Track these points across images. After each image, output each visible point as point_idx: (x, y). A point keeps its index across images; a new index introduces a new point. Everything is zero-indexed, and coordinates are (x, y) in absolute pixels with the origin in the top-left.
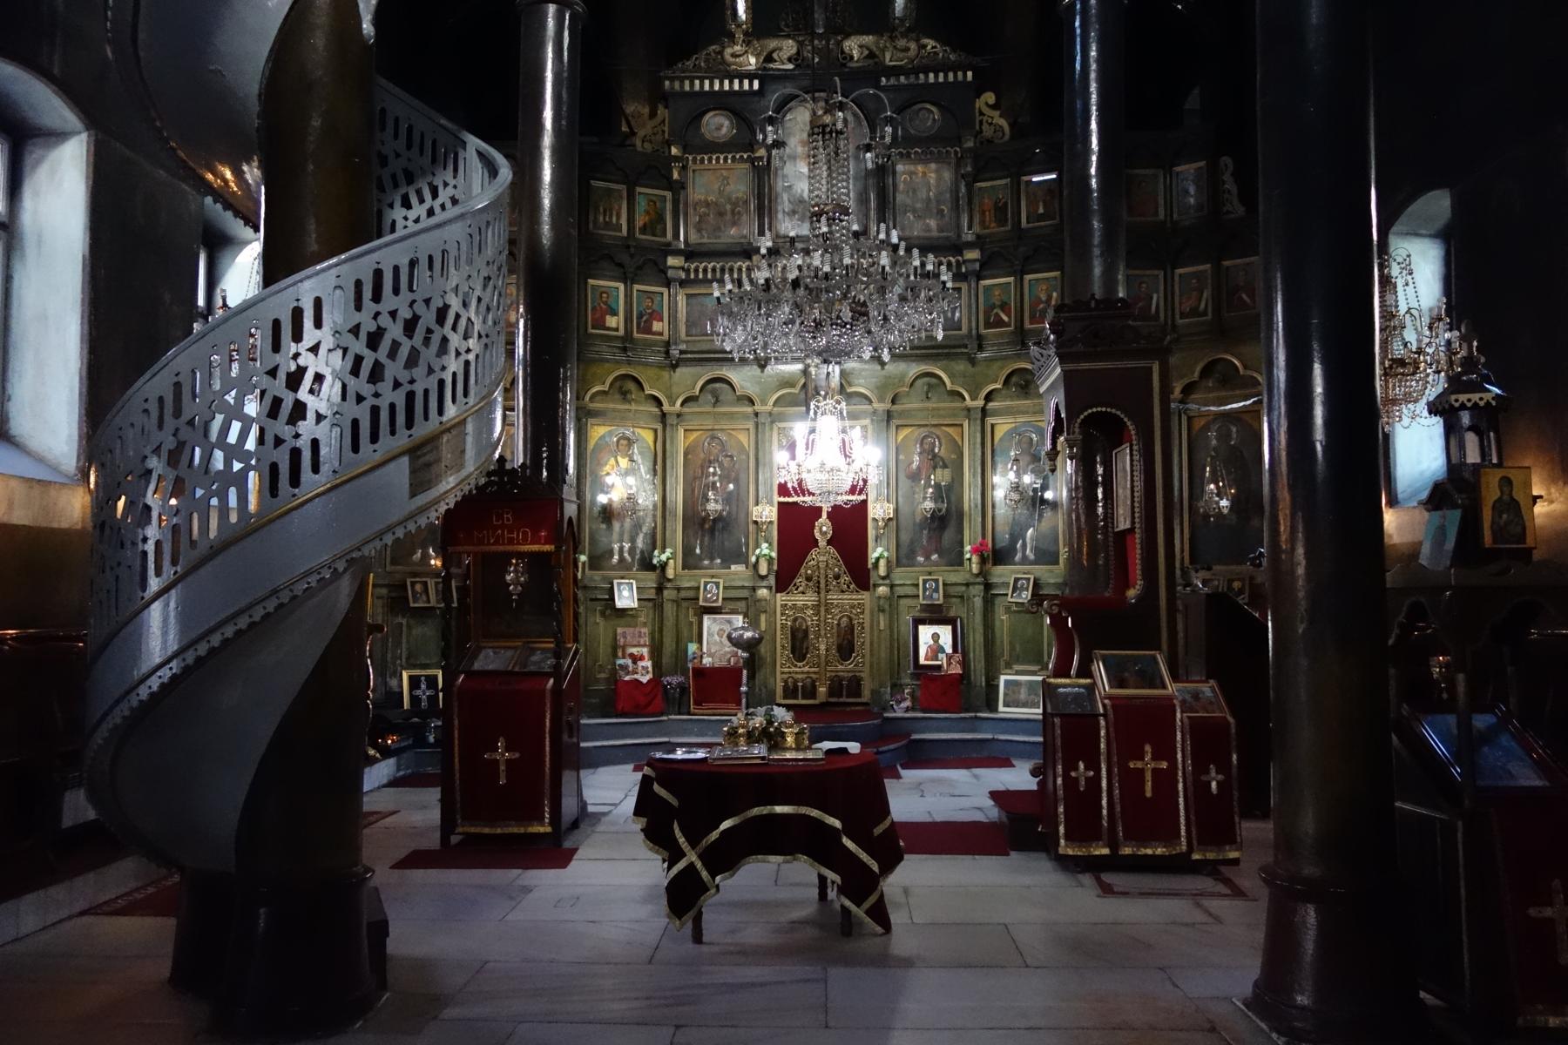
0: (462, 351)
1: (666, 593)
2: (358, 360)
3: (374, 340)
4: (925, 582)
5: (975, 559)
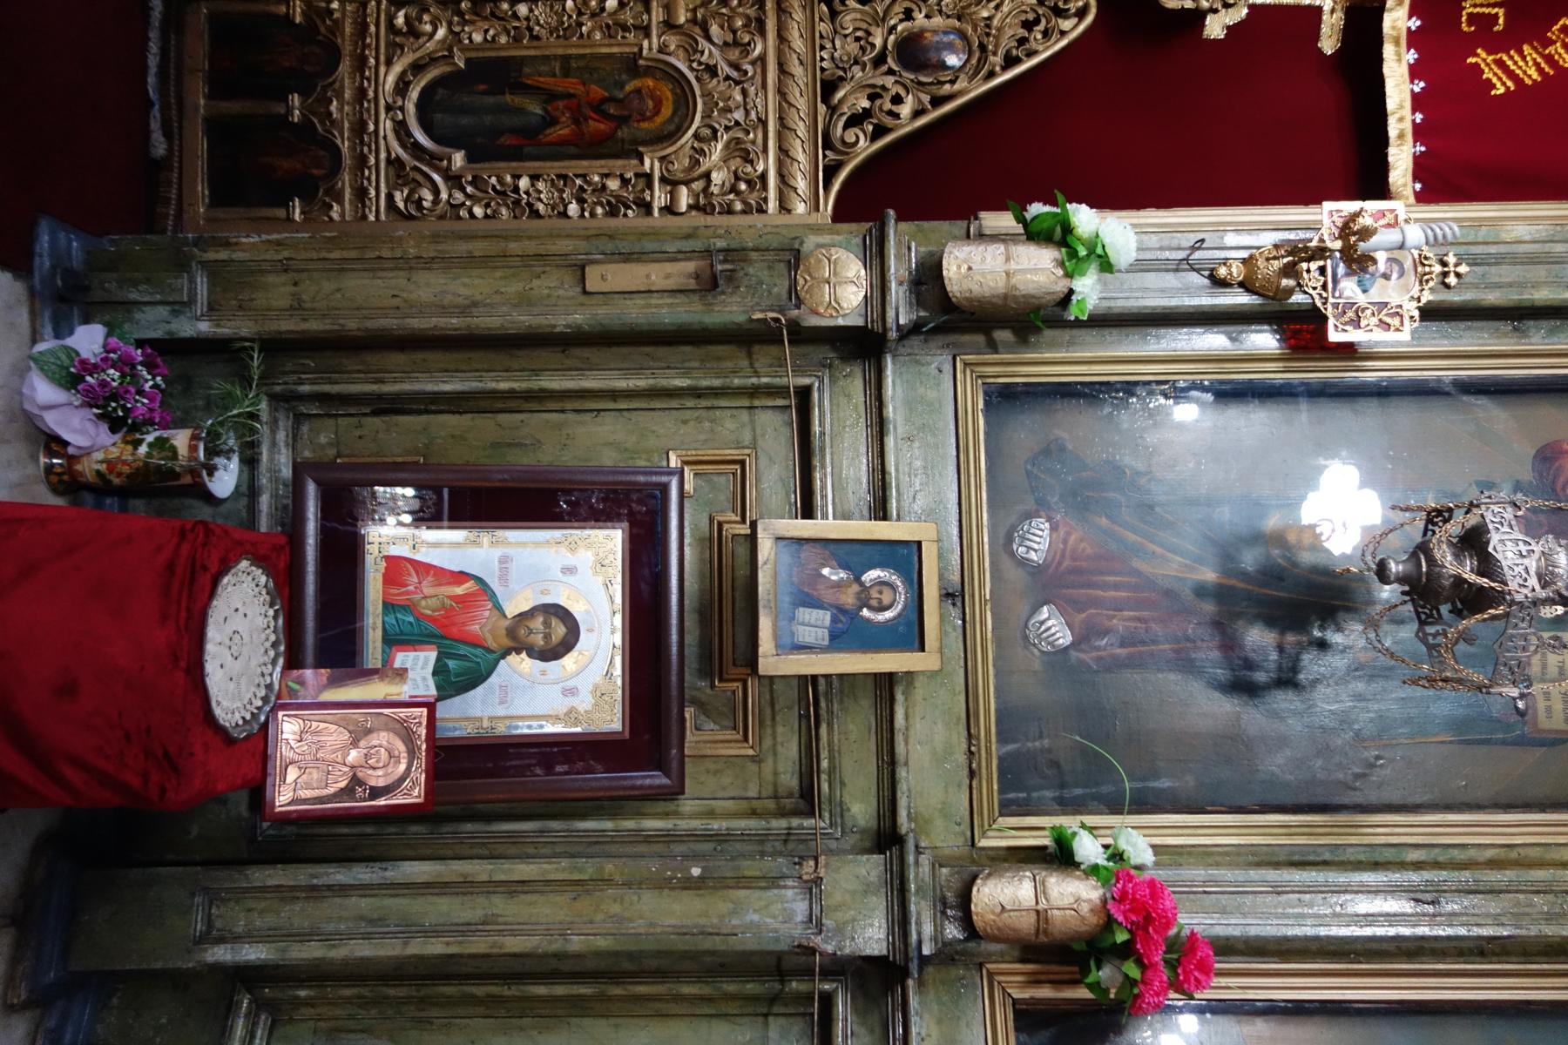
4: (904, 557)
5: (1073, 897)
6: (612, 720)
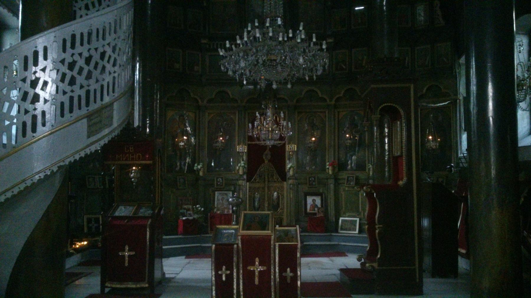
0: (112, 72)
1: (199, 182)
2: (64, 75)
3: (71, 66)
4: (310, 178)
5: (330, 168)
6: (320, 197)
